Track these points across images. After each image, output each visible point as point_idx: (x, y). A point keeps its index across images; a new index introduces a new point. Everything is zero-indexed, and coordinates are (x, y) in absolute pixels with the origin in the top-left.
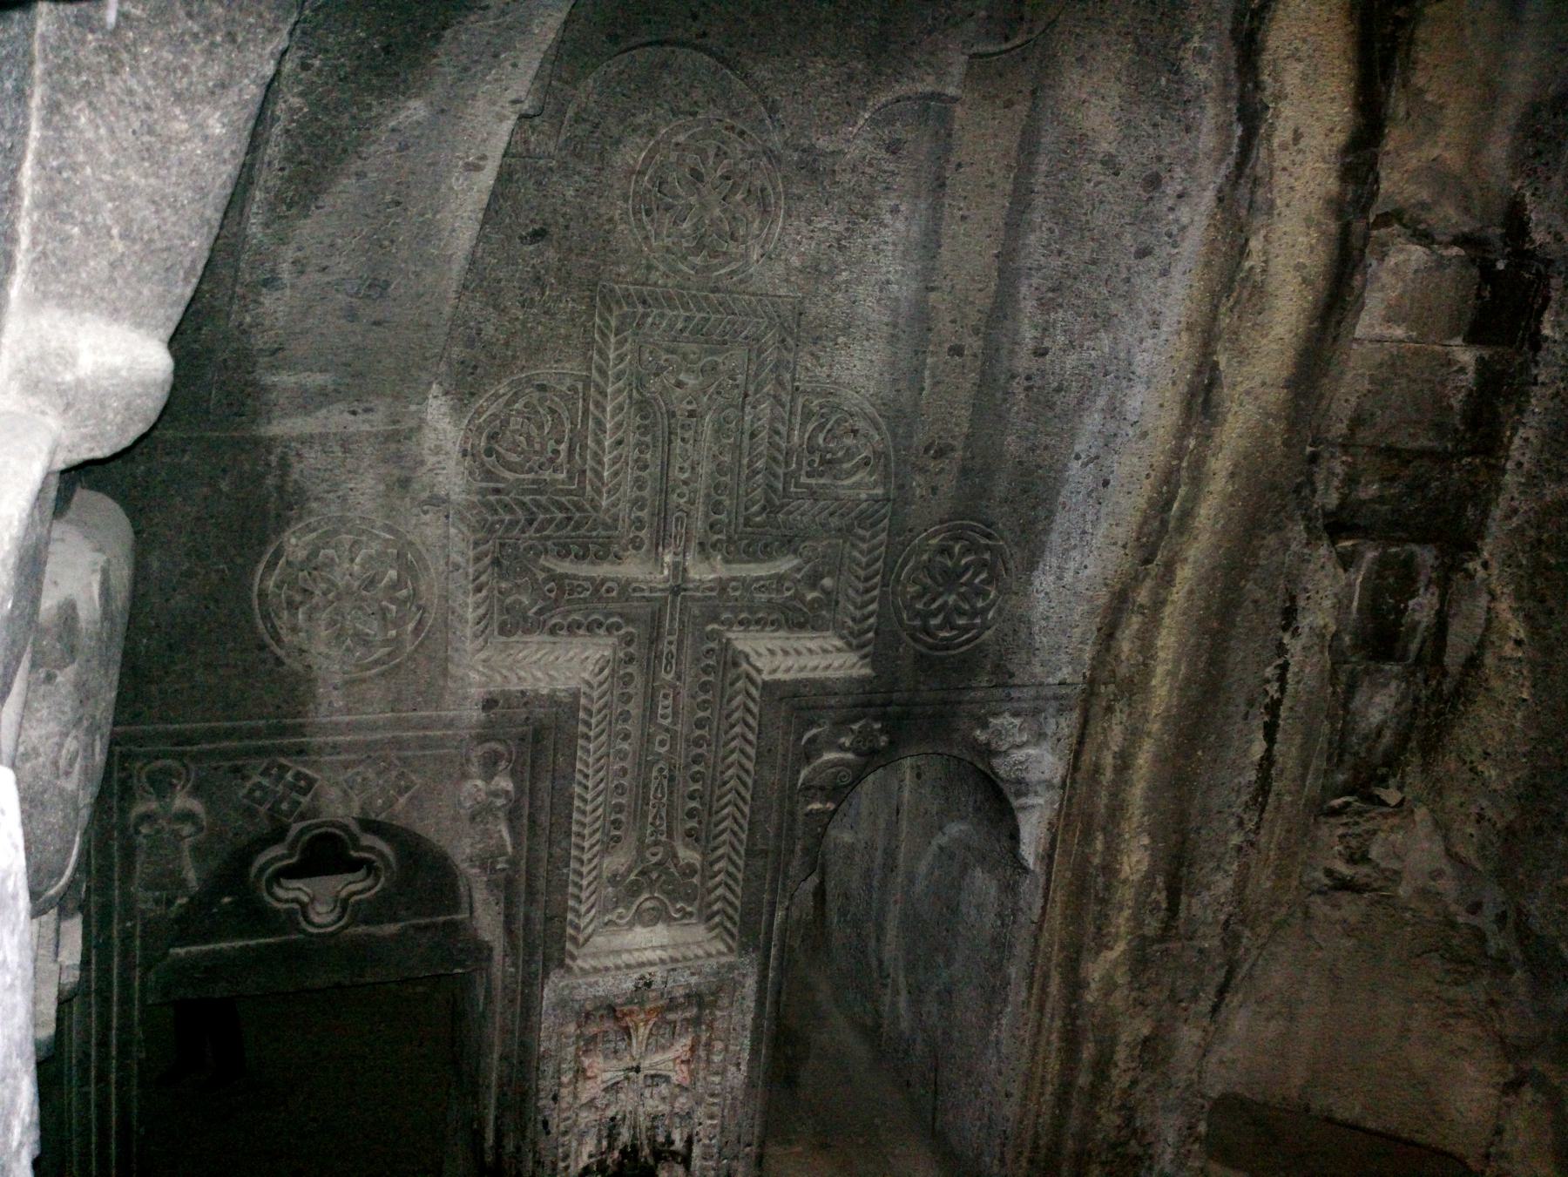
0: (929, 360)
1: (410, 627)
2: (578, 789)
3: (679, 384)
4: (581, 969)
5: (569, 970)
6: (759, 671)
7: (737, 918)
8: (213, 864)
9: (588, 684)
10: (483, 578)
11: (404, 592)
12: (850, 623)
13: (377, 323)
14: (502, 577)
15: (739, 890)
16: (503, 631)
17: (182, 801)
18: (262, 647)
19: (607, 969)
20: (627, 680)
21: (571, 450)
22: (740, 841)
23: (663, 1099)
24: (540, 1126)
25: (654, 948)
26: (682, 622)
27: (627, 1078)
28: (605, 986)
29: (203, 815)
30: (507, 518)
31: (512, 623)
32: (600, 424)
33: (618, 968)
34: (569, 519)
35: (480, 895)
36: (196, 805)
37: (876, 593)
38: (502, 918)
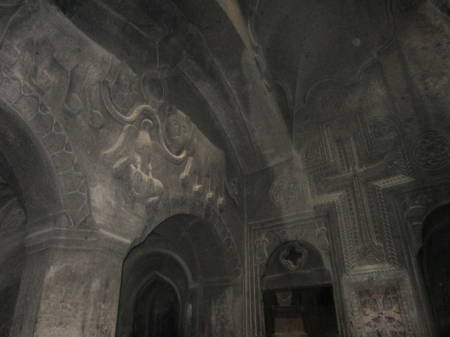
0: (396, 103)
1: (297, 194)
2: (340, 226)
3: (342, 134)
4: (352, 274)
5: (348, 274)
6: (380, 187)
7: (396, 258)
9: (336, 200)
10: (311, 183)
11: (295, 188)
12: (404, 170)
15: (394, 250)
16: (318, 194)
17: (263, 238)
19: (359, 274)
20: (349, 200)
21: (321, 152)
22: (390, 234)
23: (394, 326)
24: (350, 324)
25: (373, 269)
26: (359, 183)
27: (379, 317)
28: (359, 279)
29: (267, 241)
30: (313, 170)
31: (320, 192)
32: (326, 146)
33: (362, 274)
34: (325, 167)
35: (324, 257)
37: (407, 159)
38: (330, 263)
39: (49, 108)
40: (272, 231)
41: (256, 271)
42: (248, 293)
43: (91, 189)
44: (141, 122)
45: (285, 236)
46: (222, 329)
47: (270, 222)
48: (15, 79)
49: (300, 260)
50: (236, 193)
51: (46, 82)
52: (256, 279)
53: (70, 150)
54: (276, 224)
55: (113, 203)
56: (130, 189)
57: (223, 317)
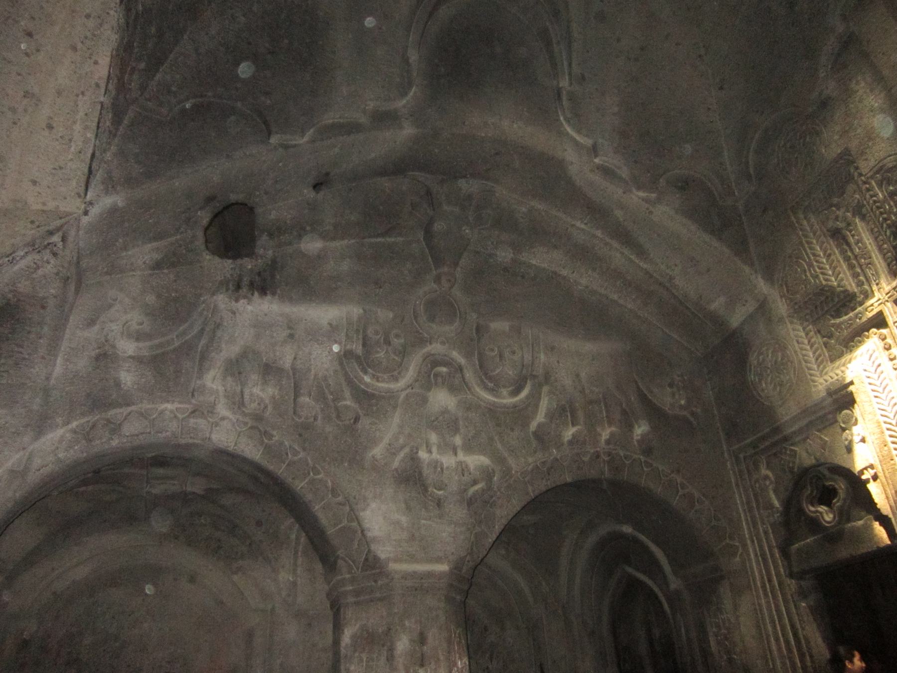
13: (708, 270)
14: (824, 337)
18: (758, 400)
32: (814, 255)
39: (275, 433)
40: (775, 454)
44: (429, 376)
45: (797, 461)
46: (730, 661)
47: (763, 438)
48: (223, 419)
49: (837, 503)
50: (683, 402)
51: (259, 404)
52: (772, 555)
53: (319, 474)
54: (776, 438)
55: (404, 519)
56: (426, 490)
57: (726, 639)
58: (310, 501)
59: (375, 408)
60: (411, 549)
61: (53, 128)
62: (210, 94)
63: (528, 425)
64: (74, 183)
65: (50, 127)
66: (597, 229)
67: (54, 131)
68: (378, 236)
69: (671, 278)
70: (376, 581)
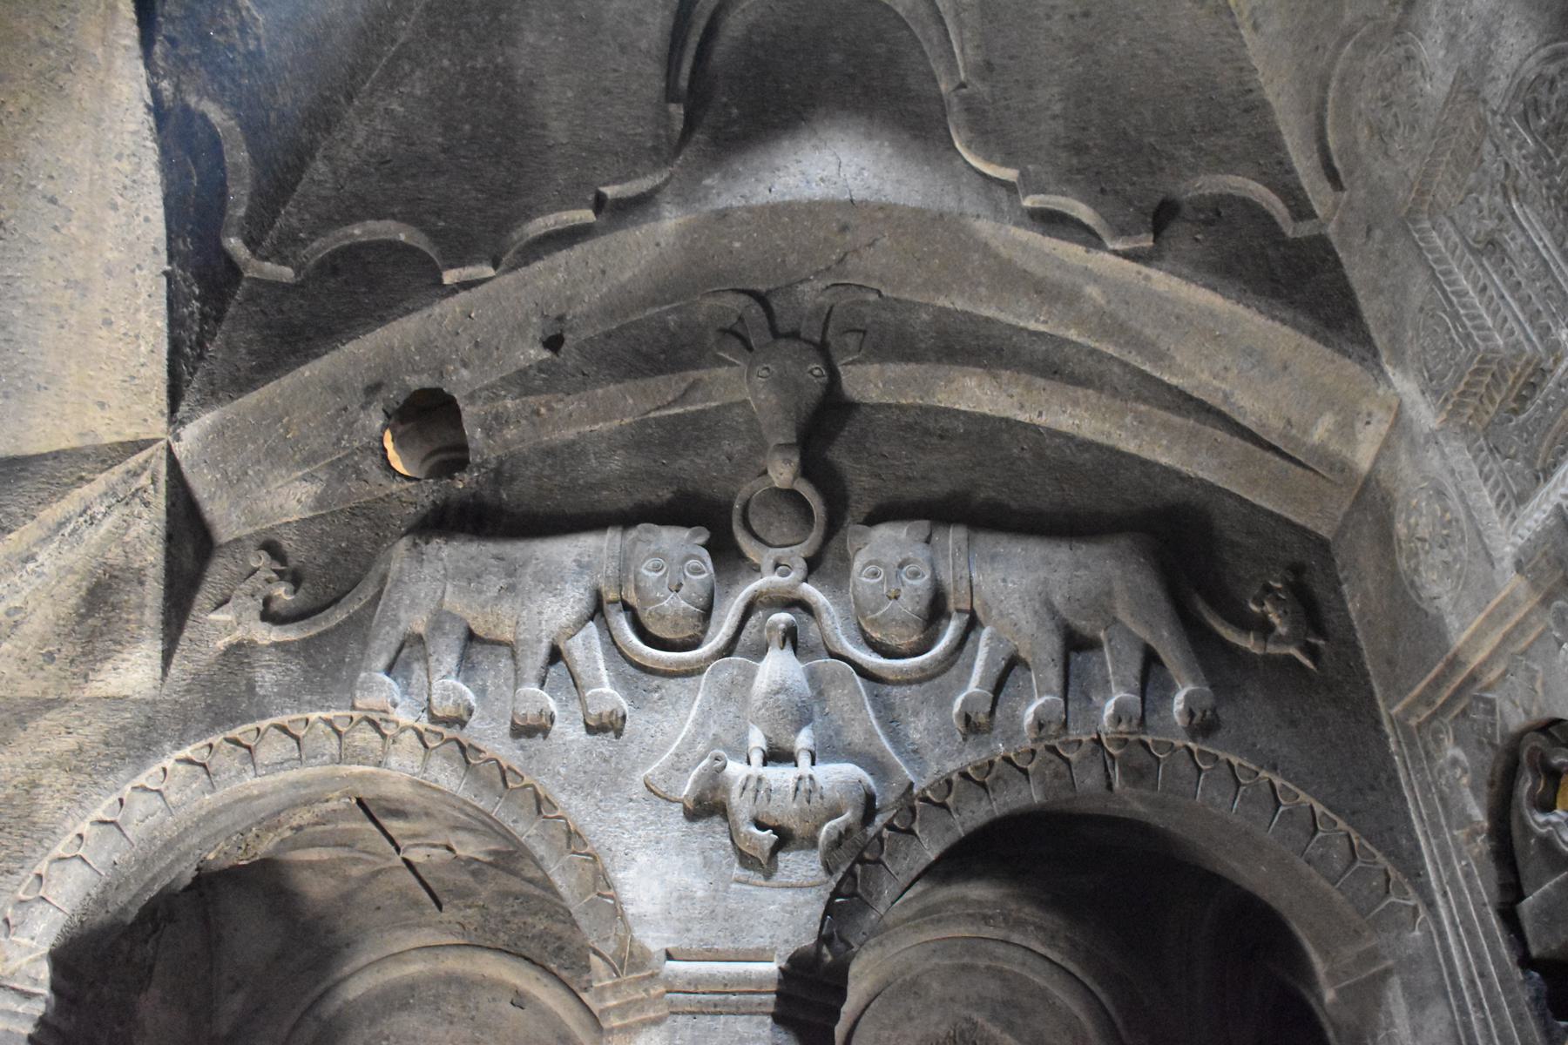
8: (1485, 800)
13: (1285, 368)
18: (1418, 608)
30: (1470, 411)
36: (1459, 753)
40: (1464, 713)
41: (1471, 891)
42: (1472, 982)
43: (620, 876)
47: (1437, 684)
52: (1483, 921)
54: (1458, 680)
58: (542, 858)
59: (656, 695)
60: (707, 935)
61: (111, 323)
62: (357, 232)
63: (950, 704)
64: (153, 396)
65: (108, 323)
66: (1068, 328)
67: (114, 327)
68: (669, 405)
69: (1226, 397)
70: (646, 990)
